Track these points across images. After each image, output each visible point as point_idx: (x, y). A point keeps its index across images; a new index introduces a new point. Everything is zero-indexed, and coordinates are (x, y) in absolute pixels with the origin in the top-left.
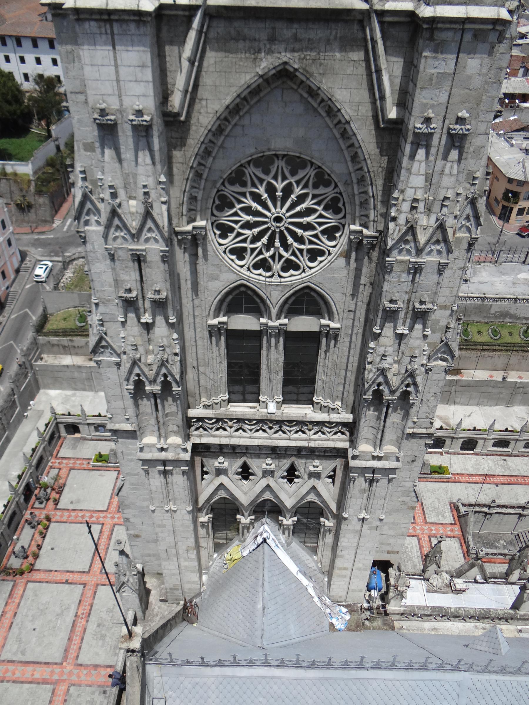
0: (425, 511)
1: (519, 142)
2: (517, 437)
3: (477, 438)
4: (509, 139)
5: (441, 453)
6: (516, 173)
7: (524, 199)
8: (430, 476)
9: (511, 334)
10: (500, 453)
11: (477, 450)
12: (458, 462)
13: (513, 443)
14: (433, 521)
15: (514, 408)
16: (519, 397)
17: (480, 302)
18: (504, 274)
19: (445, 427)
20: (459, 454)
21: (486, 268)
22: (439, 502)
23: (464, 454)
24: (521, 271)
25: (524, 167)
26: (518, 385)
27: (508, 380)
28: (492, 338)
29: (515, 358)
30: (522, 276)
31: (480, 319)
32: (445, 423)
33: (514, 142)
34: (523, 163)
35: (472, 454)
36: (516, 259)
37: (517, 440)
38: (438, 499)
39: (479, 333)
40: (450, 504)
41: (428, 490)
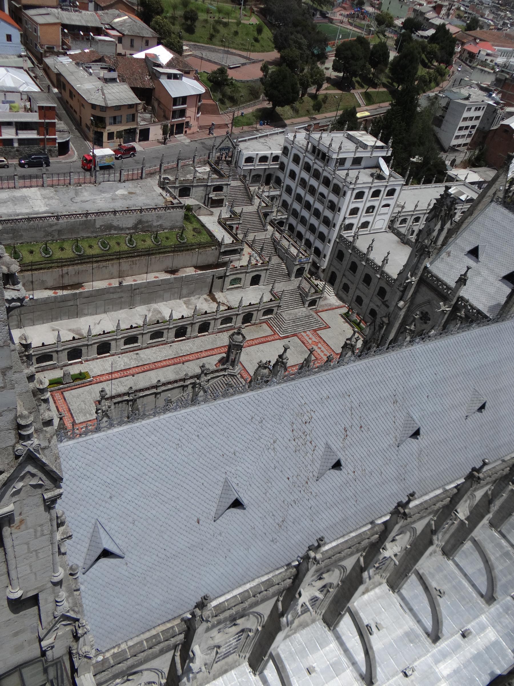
0: (74, 415)
1: (97, 71)
2: (142, 332)
3: (109, 340)
4: (86, 69)
5: (81, 363)
6: (97, 99)
7: (110, 124)
8: (73, 384)
9: (118, 244)
10: (132, 349)
11: (112, 352)
12: (96, 366)
13: (140, 337)
14: (82, 421)
15: (136, 308)
16: (138, 298)
17: (84, 219)
18: (104, 192)
19: (77, 337)
20: (97, 359)
21: (87, 188)
22: (85, 404)
23: (102, 358)
24: (118, 188)
25: (103, 94)
26: (133, 287)
27: (124, 284)
28: (103, 250)
29: (125, 265)
30: (119, 192)
31: (90, 235)
32: (77, 334)
33: (92, 71)
34: (102, 90)
35: (109, 356)
36: (112, 178)
37: (143, 334)
38: (84, 401)
39: (90, 247)
40: (95, 402)
41: (74, 397)
